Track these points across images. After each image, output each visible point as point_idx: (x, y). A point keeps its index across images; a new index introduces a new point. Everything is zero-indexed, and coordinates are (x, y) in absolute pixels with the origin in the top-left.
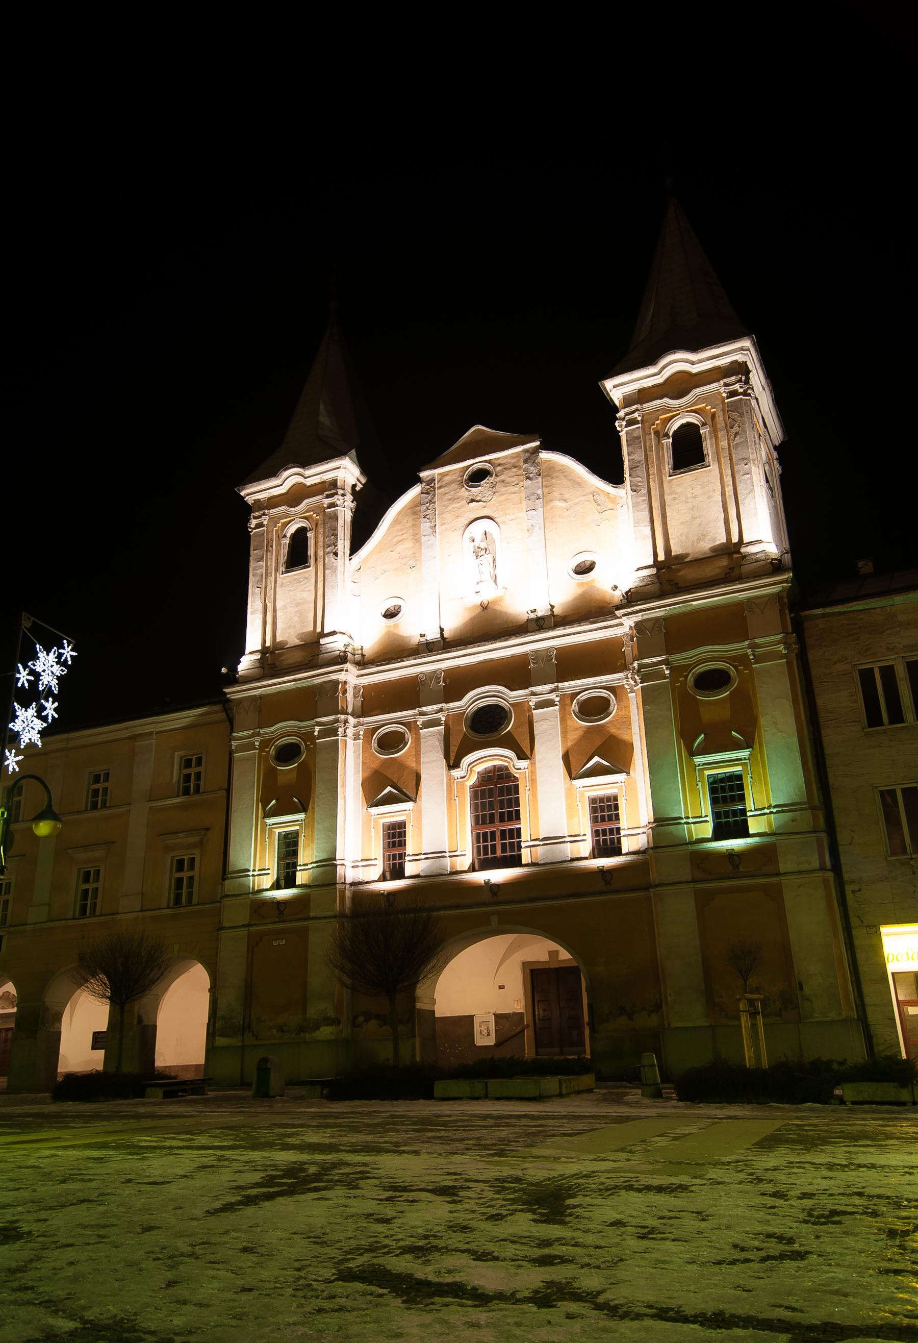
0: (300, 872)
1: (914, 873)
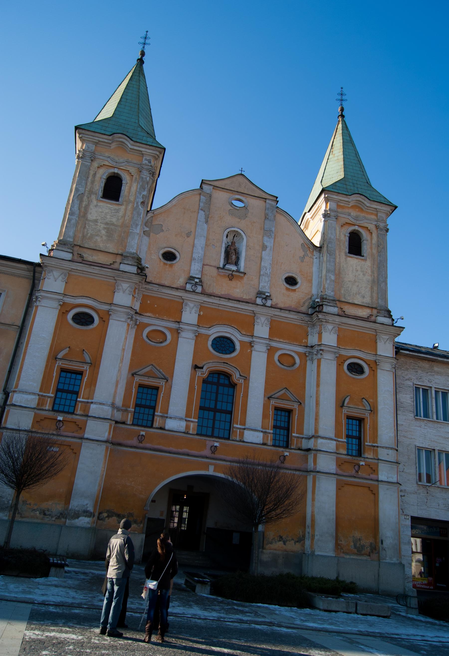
0: (80, 404)
1: (427, 493)
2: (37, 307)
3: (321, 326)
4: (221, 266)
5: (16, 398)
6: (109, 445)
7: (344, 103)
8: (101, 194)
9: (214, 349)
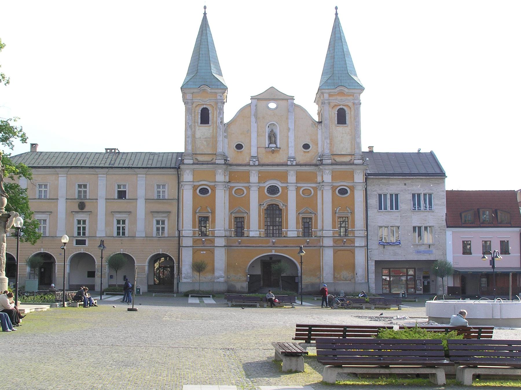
2: (183, 190)
3: (322, 171)
4: (267, 146)
5: (184, 233)
6: (226, 248)
8: (200, 121)
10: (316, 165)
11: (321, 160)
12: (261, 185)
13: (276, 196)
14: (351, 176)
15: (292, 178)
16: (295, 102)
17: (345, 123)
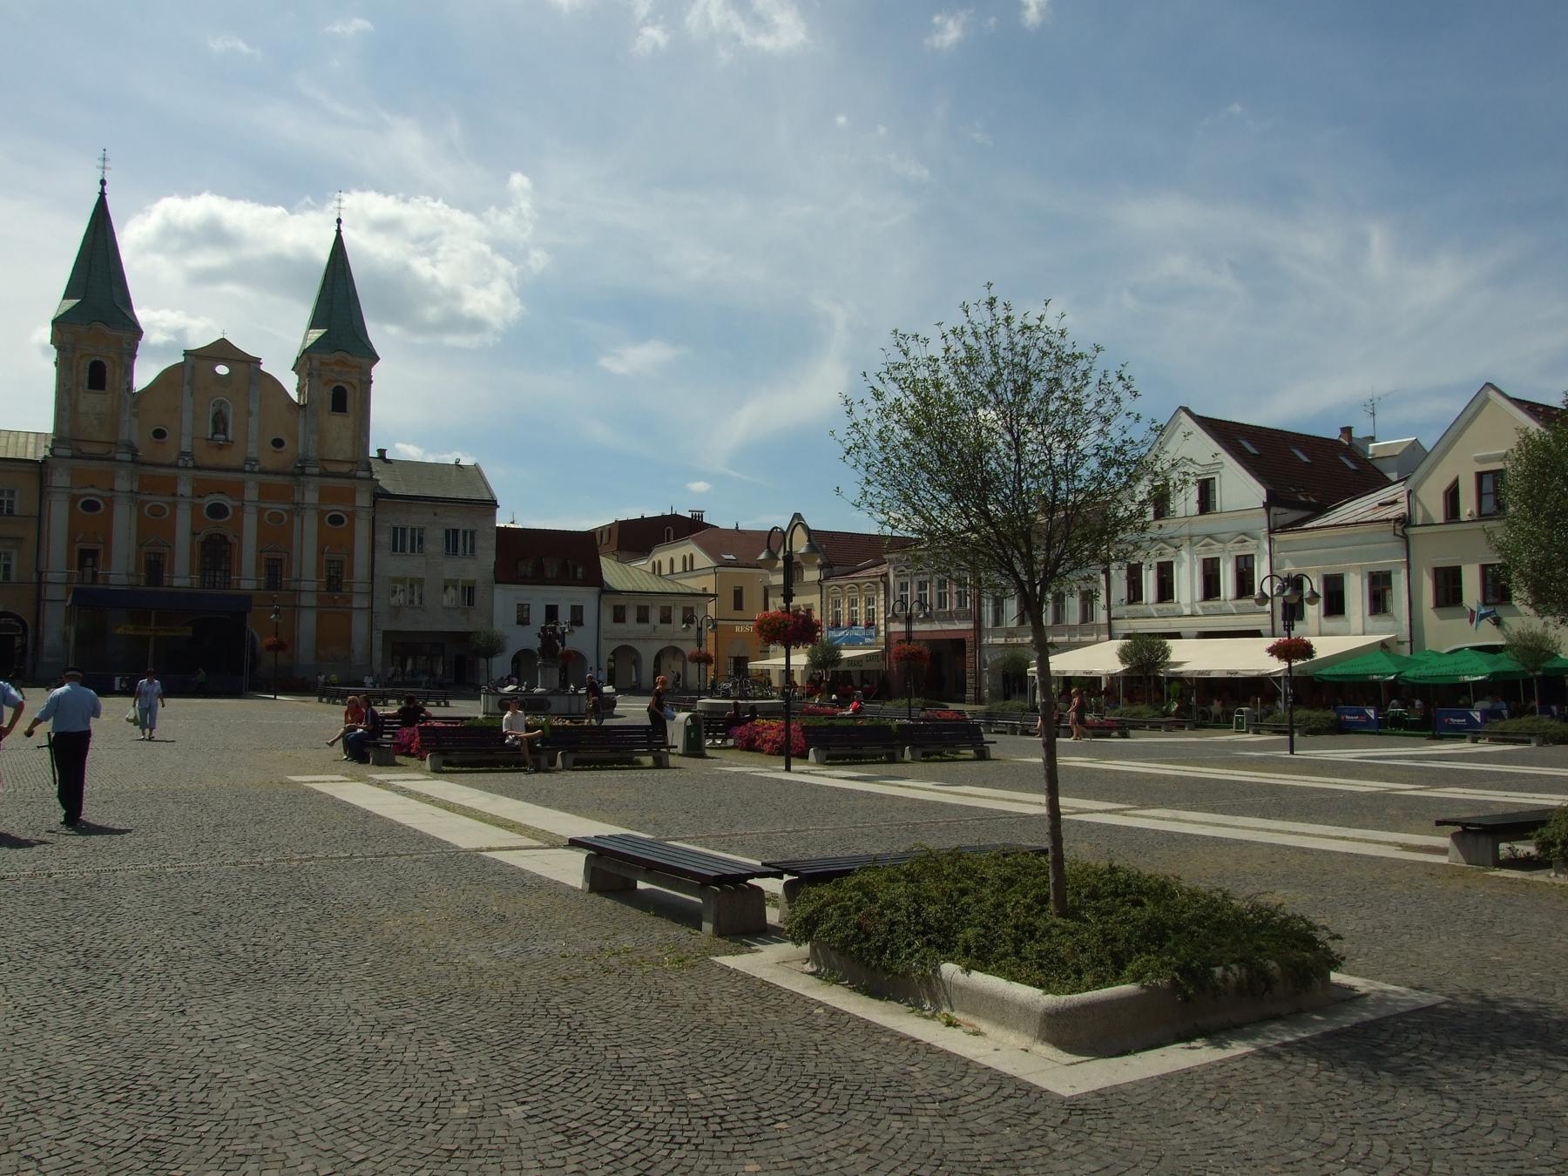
4: (210, 437)
5: (50, 577)
7: (342, 213)
8: (87, 384)
9: (209, 515)
10: (292, 474)
11: (301, 467)
12: (198, 501)
13: (222, 520)
14: (351, 496)
15: (251, 494)
16: (263, 368)
17: (345, 411)
